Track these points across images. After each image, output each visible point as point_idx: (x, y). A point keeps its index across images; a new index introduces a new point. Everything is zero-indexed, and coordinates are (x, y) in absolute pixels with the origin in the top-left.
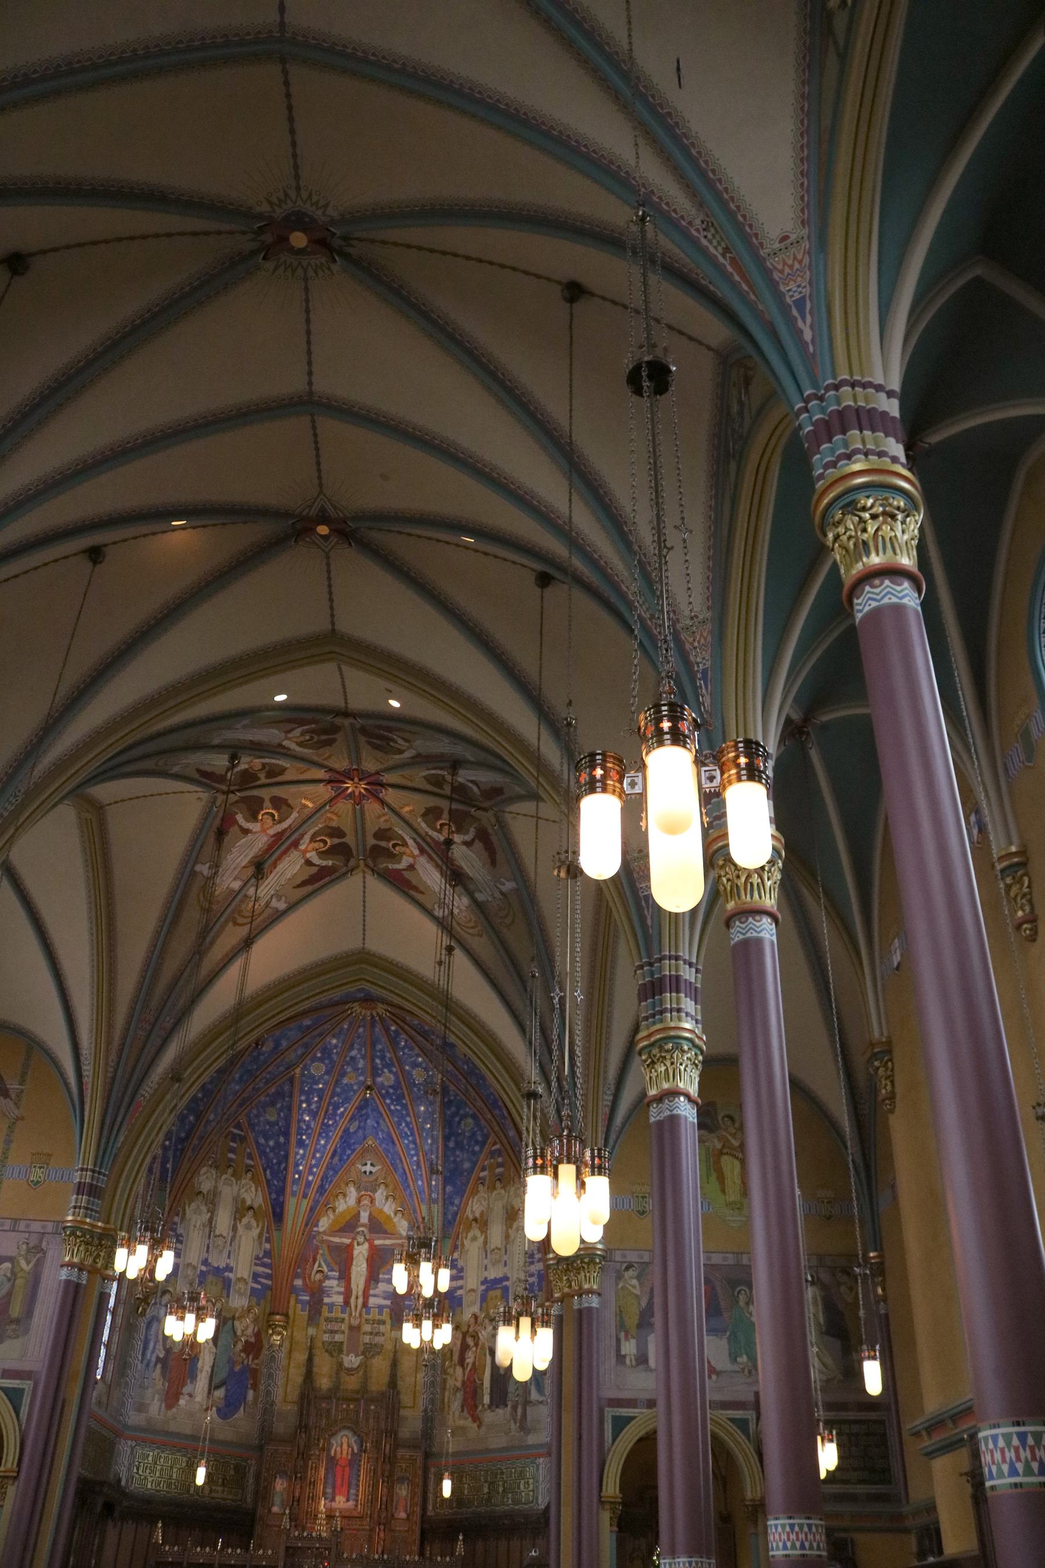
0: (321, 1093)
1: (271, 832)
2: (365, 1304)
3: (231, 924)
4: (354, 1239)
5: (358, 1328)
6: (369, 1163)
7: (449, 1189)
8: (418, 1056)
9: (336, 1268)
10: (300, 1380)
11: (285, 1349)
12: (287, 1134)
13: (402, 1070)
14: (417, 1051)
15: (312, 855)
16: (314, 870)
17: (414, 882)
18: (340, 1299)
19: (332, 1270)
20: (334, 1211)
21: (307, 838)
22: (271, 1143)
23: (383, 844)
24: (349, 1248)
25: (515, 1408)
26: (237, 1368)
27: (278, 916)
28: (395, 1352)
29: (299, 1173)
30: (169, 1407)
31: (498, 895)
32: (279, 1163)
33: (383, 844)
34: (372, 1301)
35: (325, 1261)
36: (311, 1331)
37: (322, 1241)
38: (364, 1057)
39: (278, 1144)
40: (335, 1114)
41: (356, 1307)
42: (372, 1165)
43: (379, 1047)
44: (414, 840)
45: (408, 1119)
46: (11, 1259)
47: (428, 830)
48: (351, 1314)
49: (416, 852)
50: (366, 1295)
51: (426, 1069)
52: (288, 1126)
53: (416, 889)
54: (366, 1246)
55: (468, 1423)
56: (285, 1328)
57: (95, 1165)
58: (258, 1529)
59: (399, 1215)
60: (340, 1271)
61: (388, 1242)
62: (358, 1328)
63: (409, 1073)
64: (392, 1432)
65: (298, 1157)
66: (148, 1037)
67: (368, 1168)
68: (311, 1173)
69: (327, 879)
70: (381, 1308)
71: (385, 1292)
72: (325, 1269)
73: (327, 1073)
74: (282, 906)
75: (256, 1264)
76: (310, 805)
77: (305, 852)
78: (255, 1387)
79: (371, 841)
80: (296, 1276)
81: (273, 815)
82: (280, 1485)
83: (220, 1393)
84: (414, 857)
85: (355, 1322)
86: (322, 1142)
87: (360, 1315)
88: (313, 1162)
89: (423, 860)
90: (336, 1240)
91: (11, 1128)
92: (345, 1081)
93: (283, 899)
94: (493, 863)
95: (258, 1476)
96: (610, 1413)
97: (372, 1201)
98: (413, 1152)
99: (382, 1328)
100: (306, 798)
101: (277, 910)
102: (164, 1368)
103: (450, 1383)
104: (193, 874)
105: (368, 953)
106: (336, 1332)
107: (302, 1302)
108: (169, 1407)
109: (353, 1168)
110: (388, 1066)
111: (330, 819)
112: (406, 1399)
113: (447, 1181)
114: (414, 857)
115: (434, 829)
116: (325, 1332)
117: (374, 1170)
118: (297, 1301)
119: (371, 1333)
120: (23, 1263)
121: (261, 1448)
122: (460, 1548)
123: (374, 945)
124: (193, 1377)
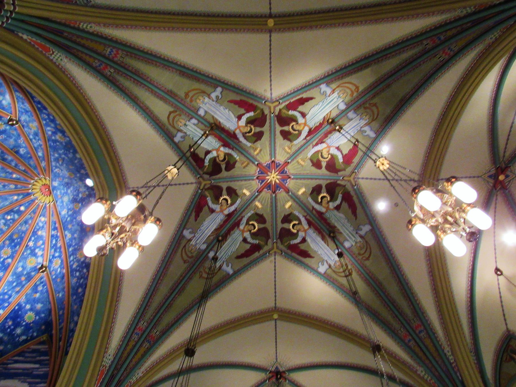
3: (172, 110)
17: (201, 214)
53: (197, 216)
57: (17, 13)
66: (104, 56)
69: (194, 163)
74: (177, 139)
76: (256, 153)
81: (249, 132)
84: (222, 211)
93: (183, 140)
100: (261, 151)
101: (176, 136)
111: (242, 164)
114: (222, 211)
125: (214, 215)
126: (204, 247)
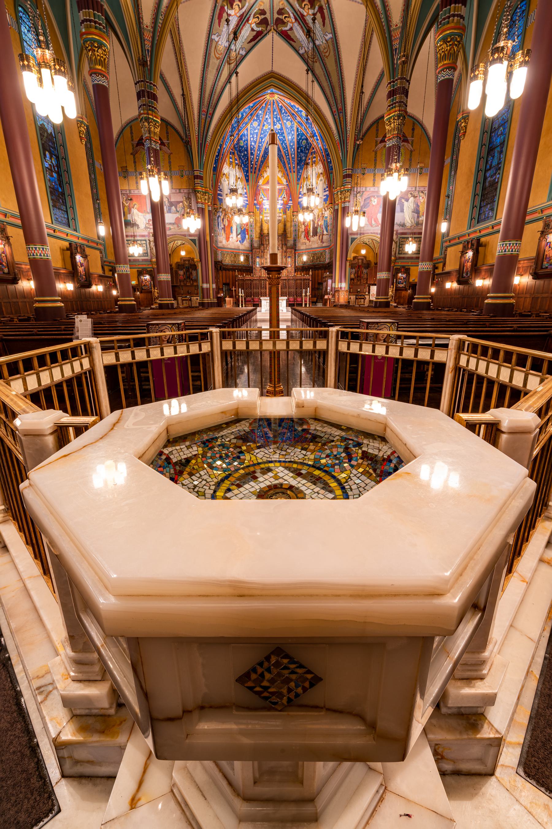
0: (257, 133)
1: (238, 15)
7: (299, 167)
8: (288, 116)
10: (259, 231)
11: (254, 223)
12: (247, 151)
13: (283, 122)
14: (288, 114)
15: (254, 25)
16: (255, 33)
17: (292, 37)
21: (252, 16)
22: (242, 154)
23: (280, 17)
25: (319, 236)
27: (243, 57)
28: (285, 222)
29: (252, 164)
30: (227, 241)
31: (324, 42)
32: (246, 161)
33: (280, 17)
36: (261, 217)
38: (270, 118)
39: (245, 155)
40: (262, 142)
43: (275, 113)
44: (293, 14)
46: (182, 202)
47: (299, 8)
49: (294, 20)
51: (291, 121)
52: (247, 148)
55: (306, 241)
58: (254, 271)
63: (285, 124)
64: (286, 244)
68: (256, 164)
69: (260, 38)
70: (280, 208)
73: (259, 125)
74: (243, 53)
77: (251, 24)
78: (248, 234)
79: (276, 16)
80: (255, 200)
81: (239, 6)
82: (258, 260)
83: (239, 236)
84: (293, 23)
89: (296, 24)
91: (169, 157)
92: (264, 128)
94: (324, 25)
95: (252, 258)
96: (350, 237)
102: (224, 231)
103: (301, 230)
104: (212, 40)
105: (274, 73)
108: (227, 241)
110: (278, 121)
111: (261, 5)
112: (289, 235)
113: (298, 164)
114: (293, 23)
115: (301, 7)
118: (256, 208)
120: (185, 203)
121: (252, 250)
122: (311, 273)
123: (276, 69)
124: (232, 232)
125: (294, 28)
126: (311, 45)
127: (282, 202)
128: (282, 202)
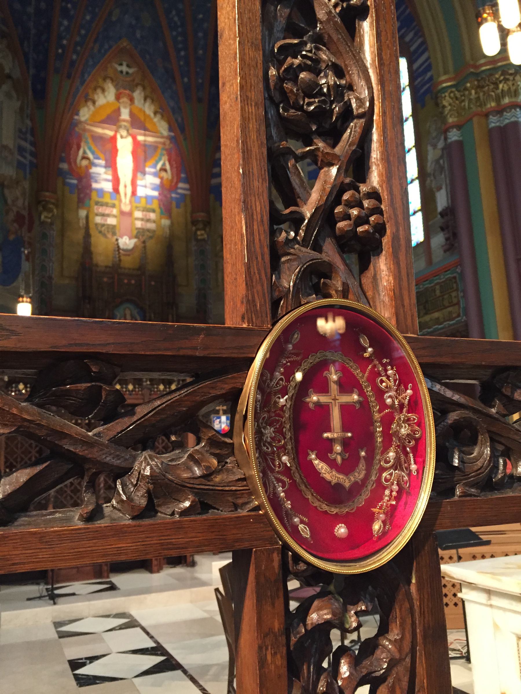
2: (134, 193)
4: (116, 132)
5: (130, 214)
6: (125, 63)
9: (102, 156)
18: (108, 187)
19: (98, 158)
20: (94, 102)
24: (113, 139)
26: (12, 237)
29: (62, 47)
34: (141, 192)
35: (90, 149)
37: (85, 130)
41: (126, 195)
42: (128, 66)
45: (180, 6)
48: (120, 201)
50: (134, 183)
54: (130, 140)
56: (57, 206)
59: (159, 116)
60: (106, 160)
61: (150, 139)
62: (130, 214)
65: (62, 28)
67: (124, 68)
71: (151, 184)
72: (91, 156)
75: (19, 137)
80: (62, 160)
85: (126, 208)
86: (88, 18)
87: (131, 202)
88: (78, 39)
90: (99, 130)
97: (132, 100)
98: (180, 46)
99: (152, 216)
106: (108, 215)
107: (70, 185)
109: (109, 65)
116: (97, 215)
117: (131, 71)
119: (142, 220)
127: (157, 181)
128: (157, 181)
